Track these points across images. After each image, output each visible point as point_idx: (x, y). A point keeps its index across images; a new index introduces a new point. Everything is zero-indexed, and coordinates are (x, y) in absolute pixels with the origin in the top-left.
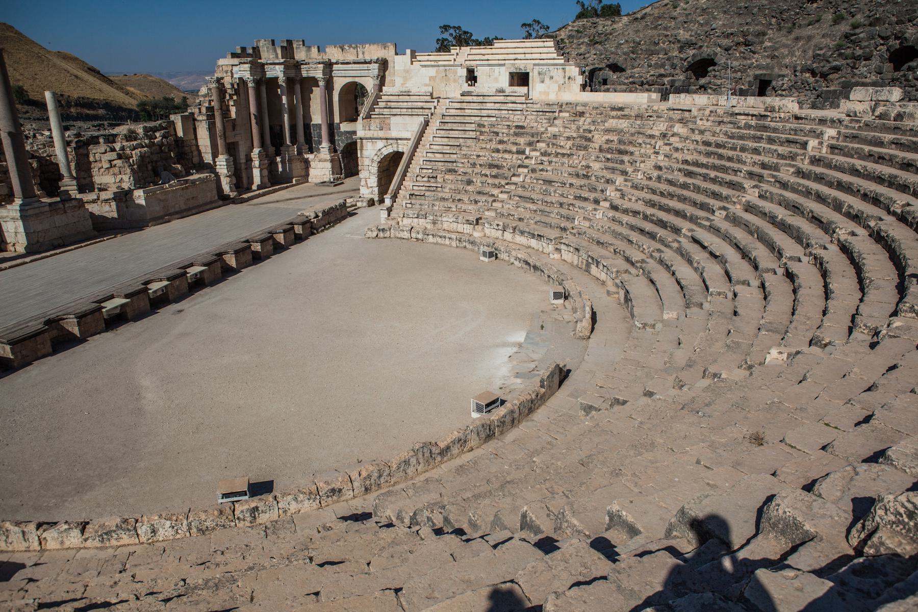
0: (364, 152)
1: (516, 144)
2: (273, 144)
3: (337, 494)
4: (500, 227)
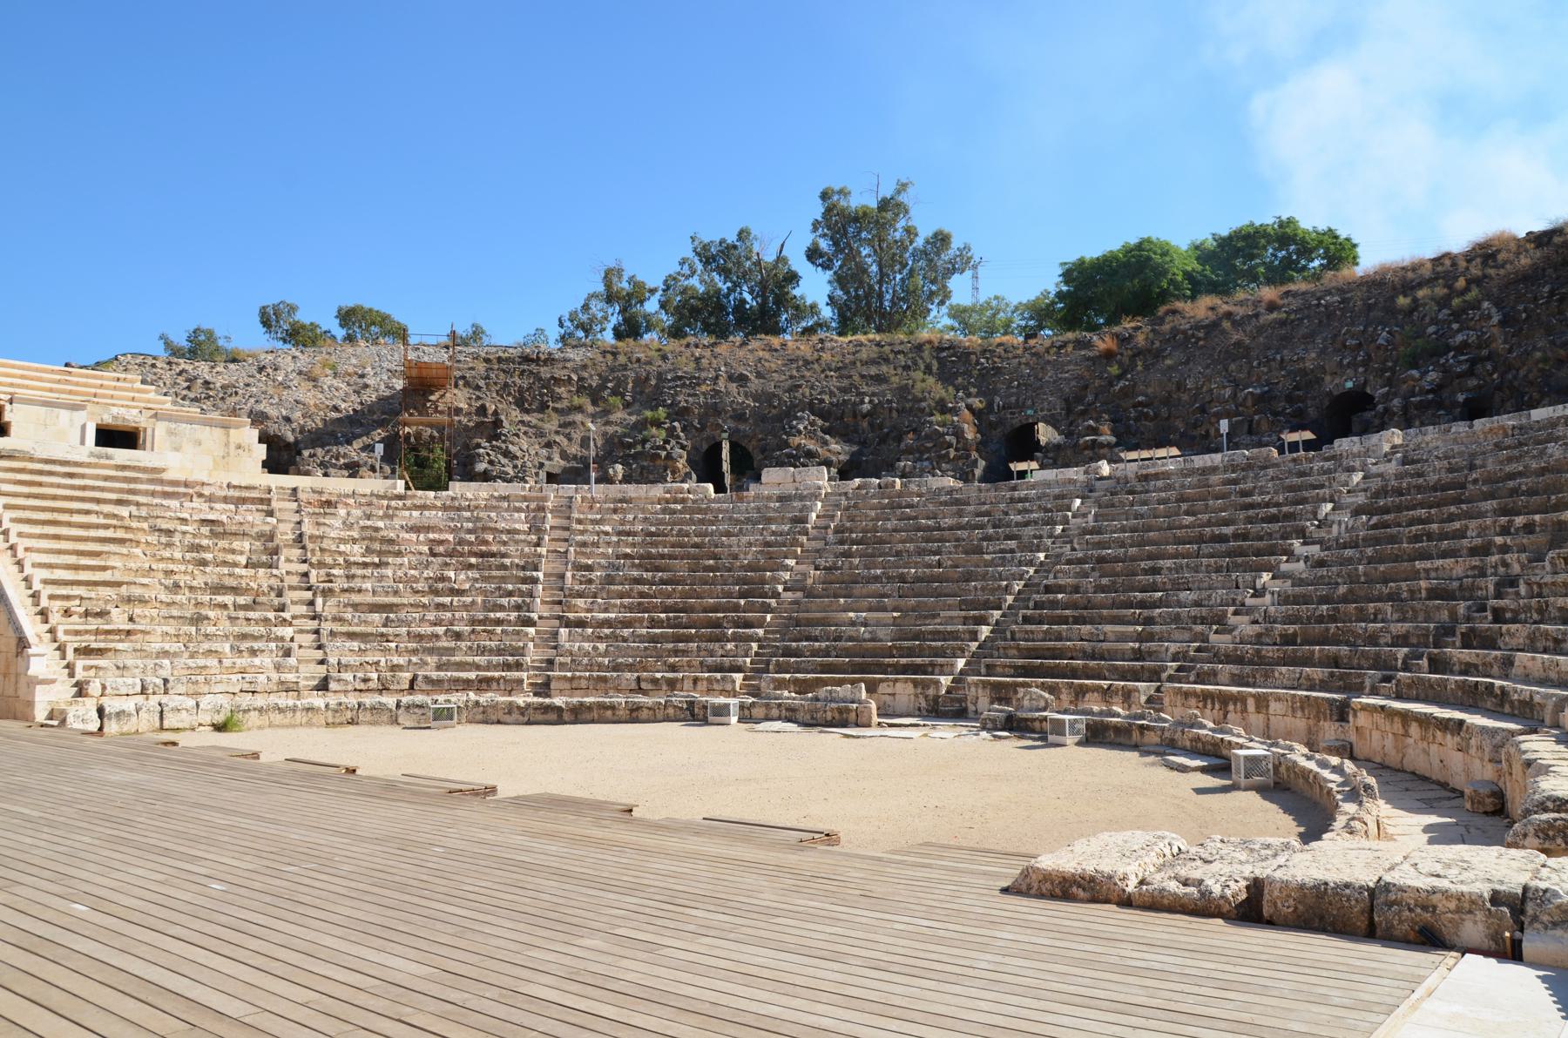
1: (233, 552)
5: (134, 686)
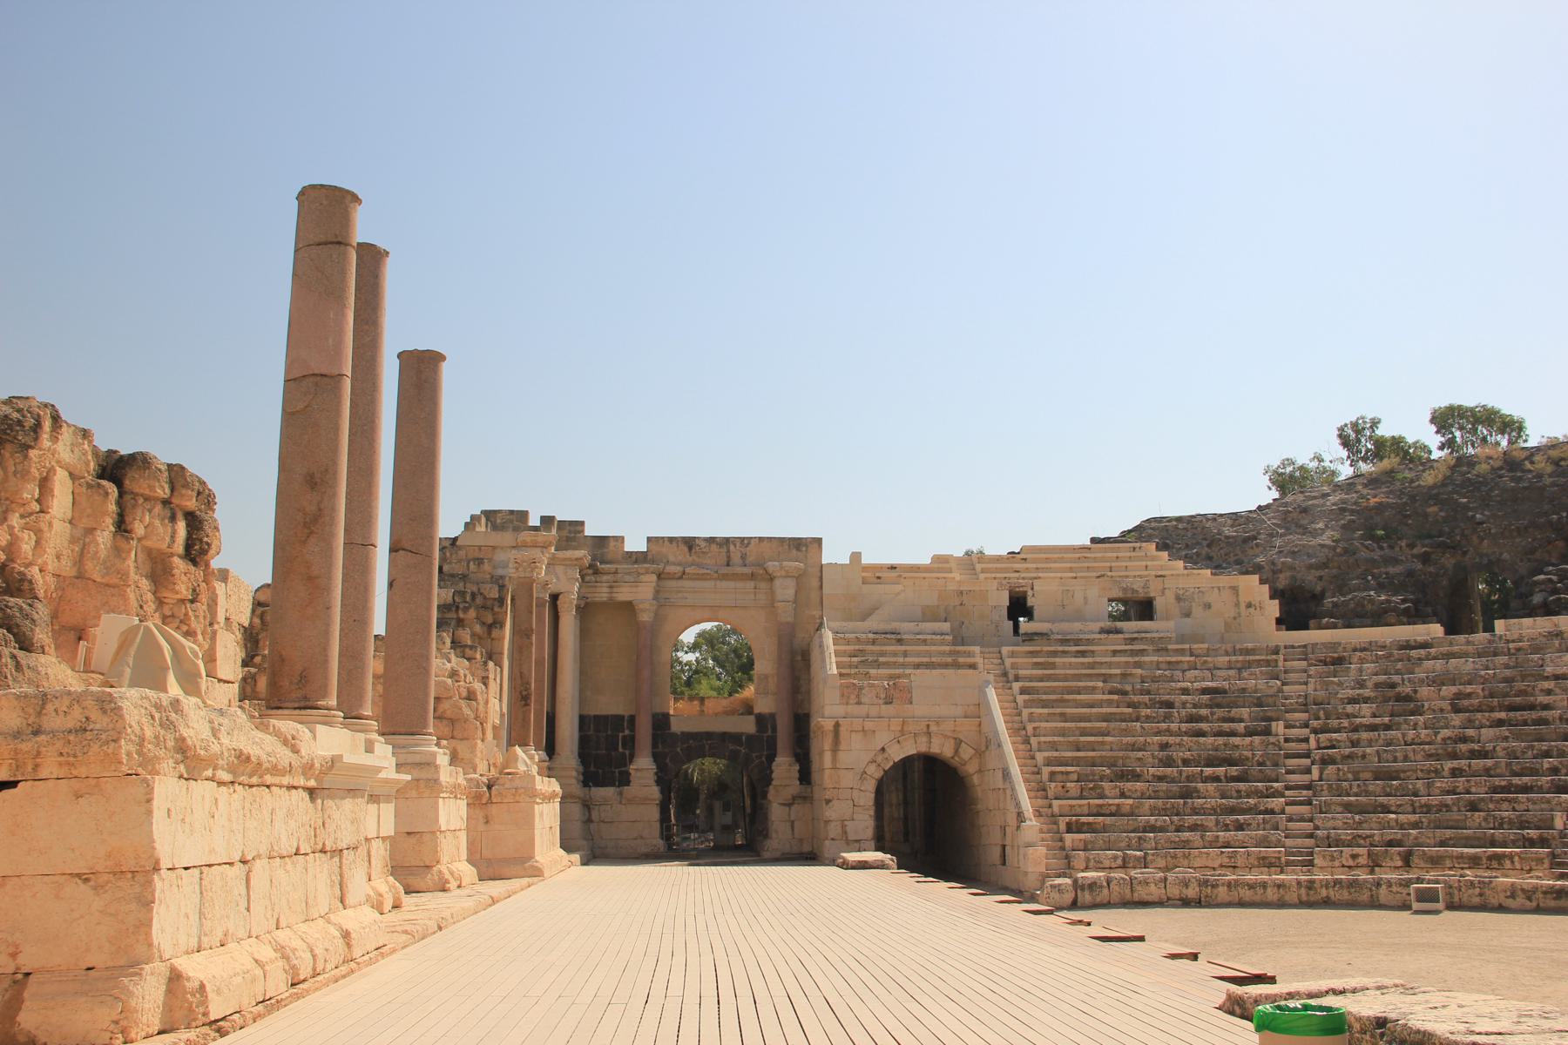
0: (841, 755)
1: (1232, 720)
5: (1115, 858)
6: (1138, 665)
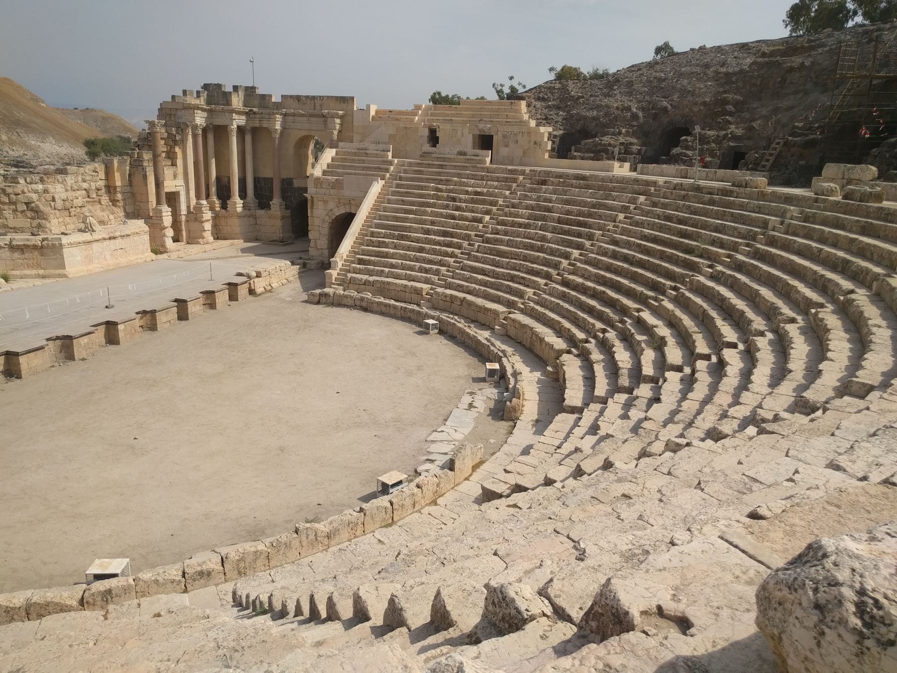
1: (473, 212)
2: (219, 197)
3: (205, 577)
4: (448, 299)
6: (459, 176)
